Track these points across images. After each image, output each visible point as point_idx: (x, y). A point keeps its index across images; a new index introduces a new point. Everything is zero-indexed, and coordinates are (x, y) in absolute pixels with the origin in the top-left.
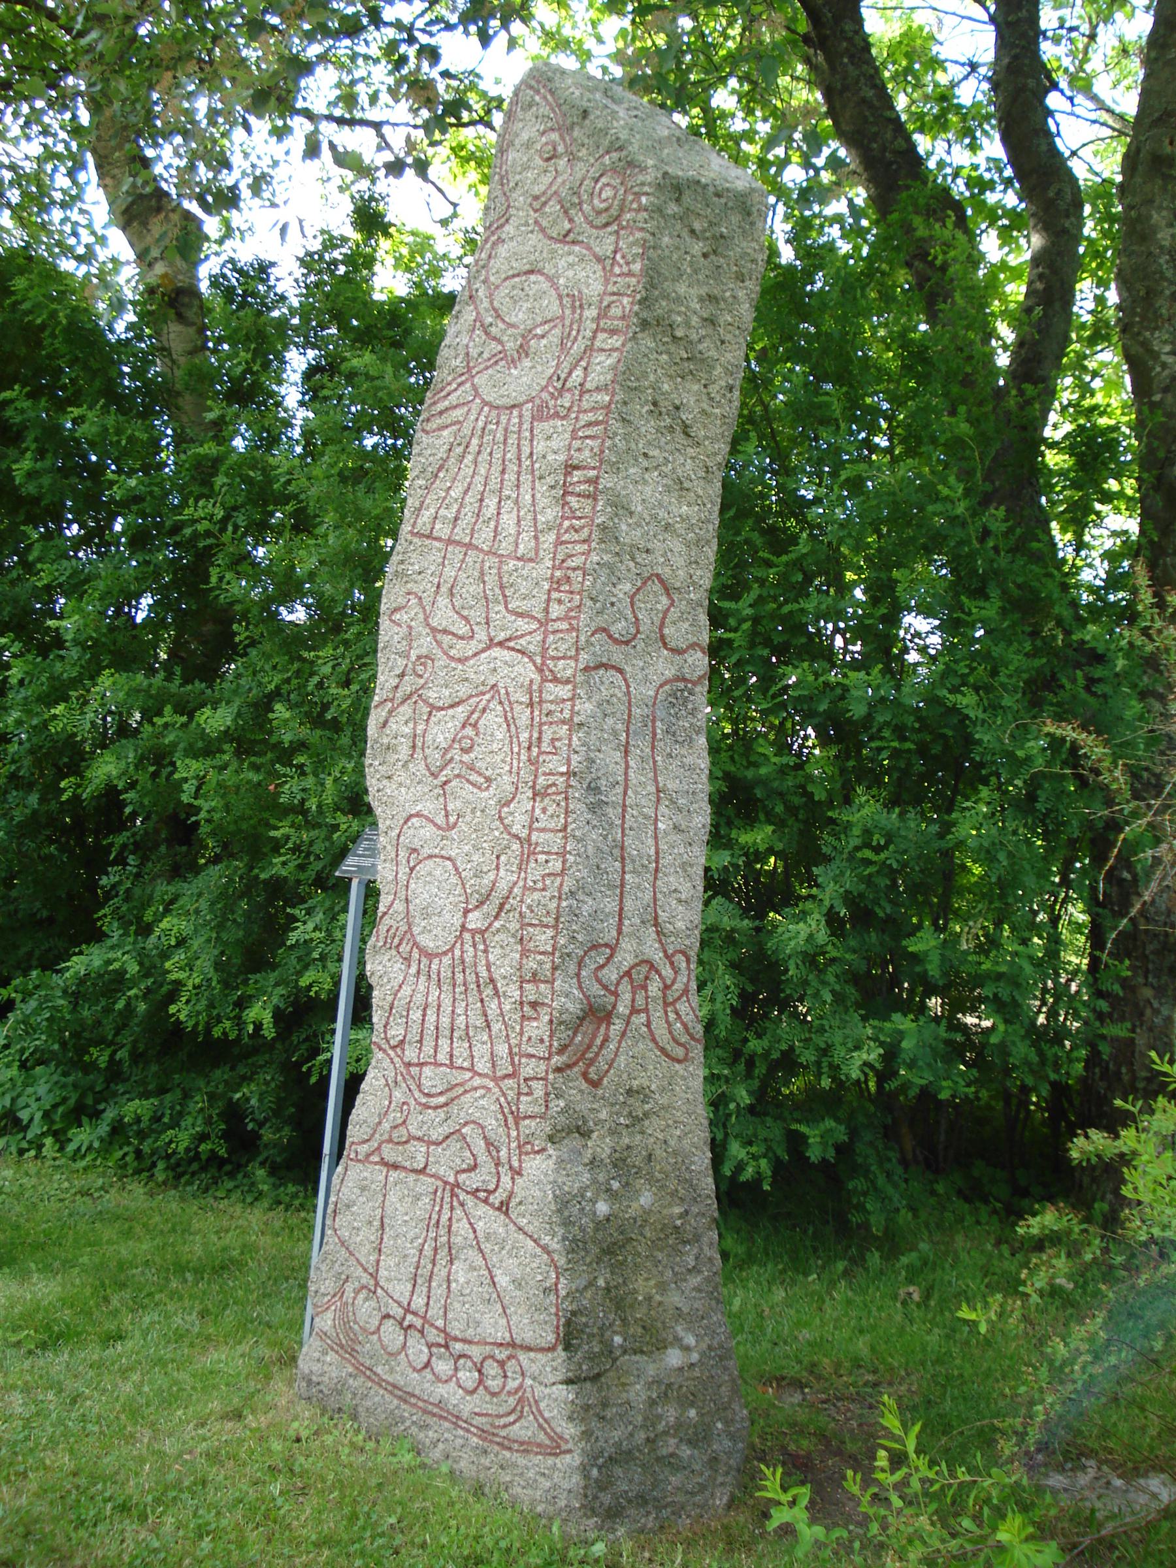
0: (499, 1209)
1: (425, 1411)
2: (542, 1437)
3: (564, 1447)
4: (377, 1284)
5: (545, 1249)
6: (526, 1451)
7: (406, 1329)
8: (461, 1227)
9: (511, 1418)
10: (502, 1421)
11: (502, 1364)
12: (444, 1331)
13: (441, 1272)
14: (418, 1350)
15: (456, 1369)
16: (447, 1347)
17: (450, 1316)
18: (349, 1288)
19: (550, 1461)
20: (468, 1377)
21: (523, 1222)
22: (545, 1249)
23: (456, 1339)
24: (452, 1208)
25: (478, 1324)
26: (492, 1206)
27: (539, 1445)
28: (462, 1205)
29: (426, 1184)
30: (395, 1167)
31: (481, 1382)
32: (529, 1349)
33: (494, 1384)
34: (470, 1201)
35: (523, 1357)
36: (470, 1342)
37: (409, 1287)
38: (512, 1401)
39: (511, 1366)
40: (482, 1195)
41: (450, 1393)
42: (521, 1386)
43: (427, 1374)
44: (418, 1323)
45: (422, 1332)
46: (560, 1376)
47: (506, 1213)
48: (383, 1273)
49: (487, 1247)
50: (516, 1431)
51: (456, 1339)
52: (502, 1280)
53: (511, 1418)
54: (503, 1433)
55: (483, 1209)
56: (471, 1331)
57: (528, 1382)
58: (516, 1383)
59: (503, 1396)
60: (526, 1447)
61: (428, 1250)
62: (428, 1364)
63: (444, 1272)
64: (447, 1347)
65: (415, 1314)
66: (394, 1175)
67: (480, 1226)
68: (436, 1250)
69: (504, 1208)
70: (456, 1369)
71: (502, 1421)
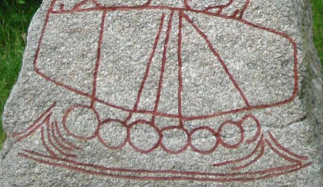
0: (233, 17)
1: (157, 179)
2: (283, 161)
3: (304, 162)
4: (94, 99)
5: (285, 35)
6: (269, 176)
7: (129, 127)
8: (191, 38)
9: (252, 158)
10: (243, 163)
11: (239, 124)
12: (180, 116)
13: (171, 75)
14: (144, 136)
15: (189, 139)
16: (181, 126)
17: (184, 103)
18: (57, 113)
19: (292, 176)
20: (203, 141)
21: (257, 21)
22: (285, 35)
23: (192, 118)
24: (180, 26)
25: (212, 102)
26: (224, 16)
27: (280, 168)
28: (191, 22)
29: (152, 15)
30: (113, 8)
31: (219, 141)
32: (267, 106)
33: (231, 140)
34: (200, 17)
35: (259, 114)
36: (206, 117)
37: (135, 93)
38: (252, 146)
39: (248, 123)
40: (214, 10)
41: (190, 159)
42: (258, 134)
43: (159, 151)
44: (148, 117)
45: (151, 123)
46: (296, 117)
47: (240, 19)
48: (101, 92)
49: (218, 47)
50: (260, 164)
51: (192, 118)
52: (236, 66)
53: (252, 158)
54: (243, 171)
55: (213, 20)
56: (206, 109)
57: (264, 129)
58: (254, 133)
59: (242, 145)
60: (266, 174)
61: (156, 62)
62: (159, 144)
63: (174, 75)
64: (181, 126)
65: (141, 111)
66: (110, 16)
67: (212, 34)
68: (164, 60)
69: (238, 16)
70: (189, 139)
71: (243, 163)
